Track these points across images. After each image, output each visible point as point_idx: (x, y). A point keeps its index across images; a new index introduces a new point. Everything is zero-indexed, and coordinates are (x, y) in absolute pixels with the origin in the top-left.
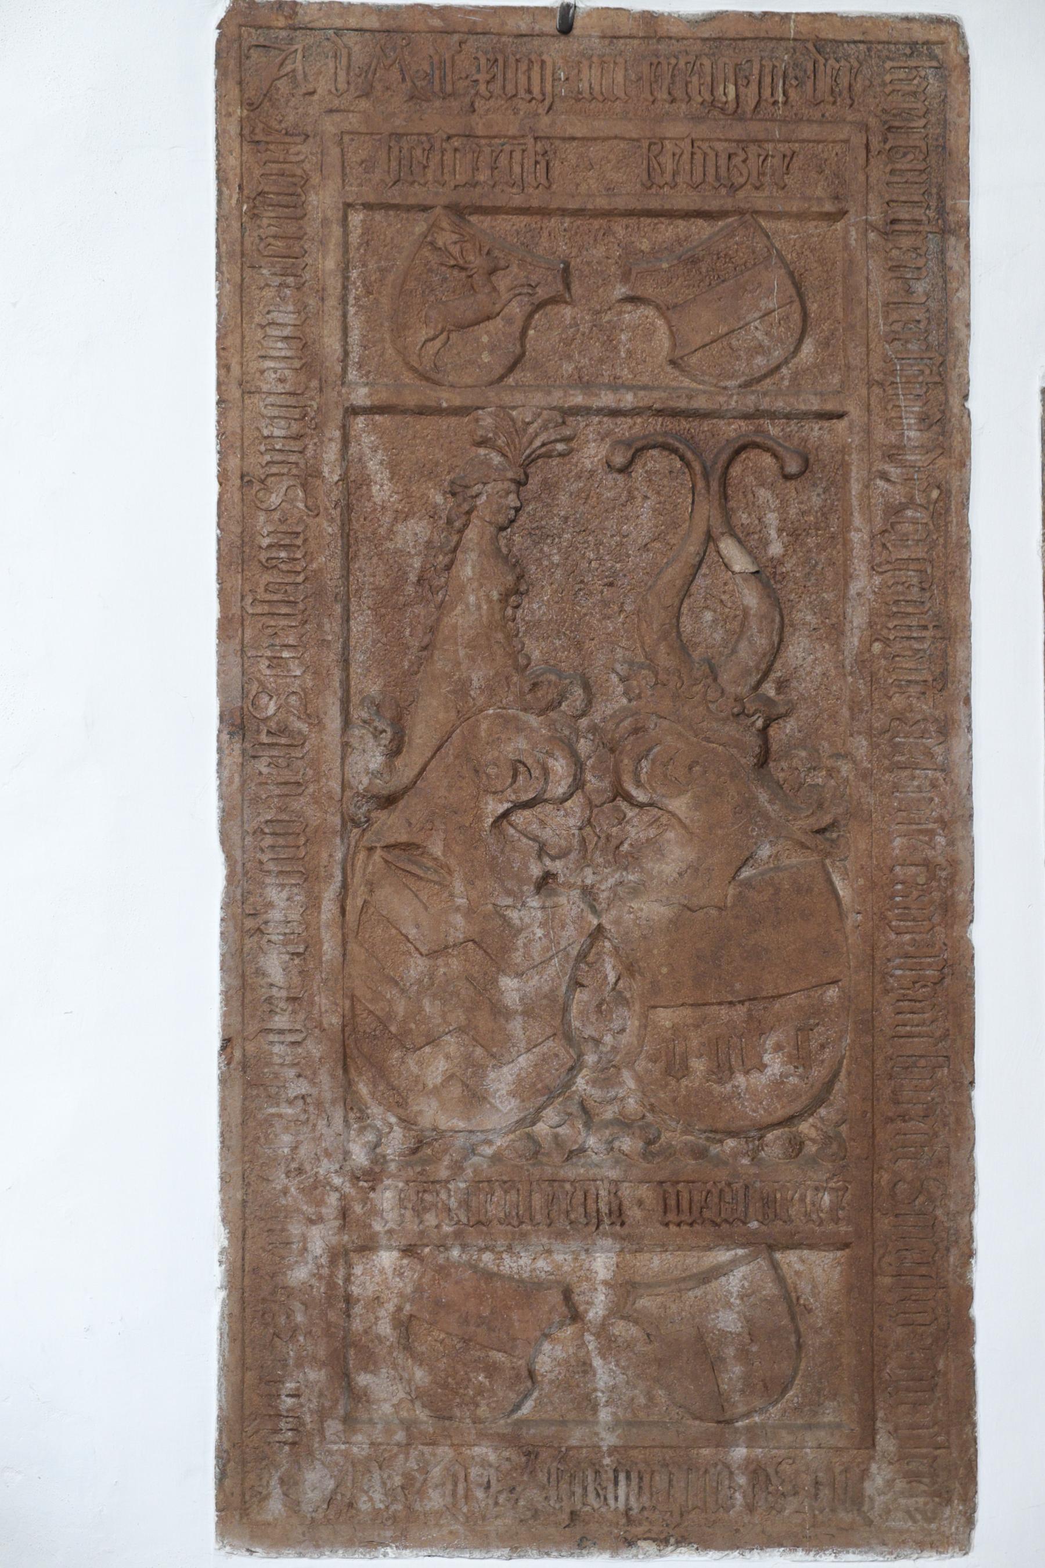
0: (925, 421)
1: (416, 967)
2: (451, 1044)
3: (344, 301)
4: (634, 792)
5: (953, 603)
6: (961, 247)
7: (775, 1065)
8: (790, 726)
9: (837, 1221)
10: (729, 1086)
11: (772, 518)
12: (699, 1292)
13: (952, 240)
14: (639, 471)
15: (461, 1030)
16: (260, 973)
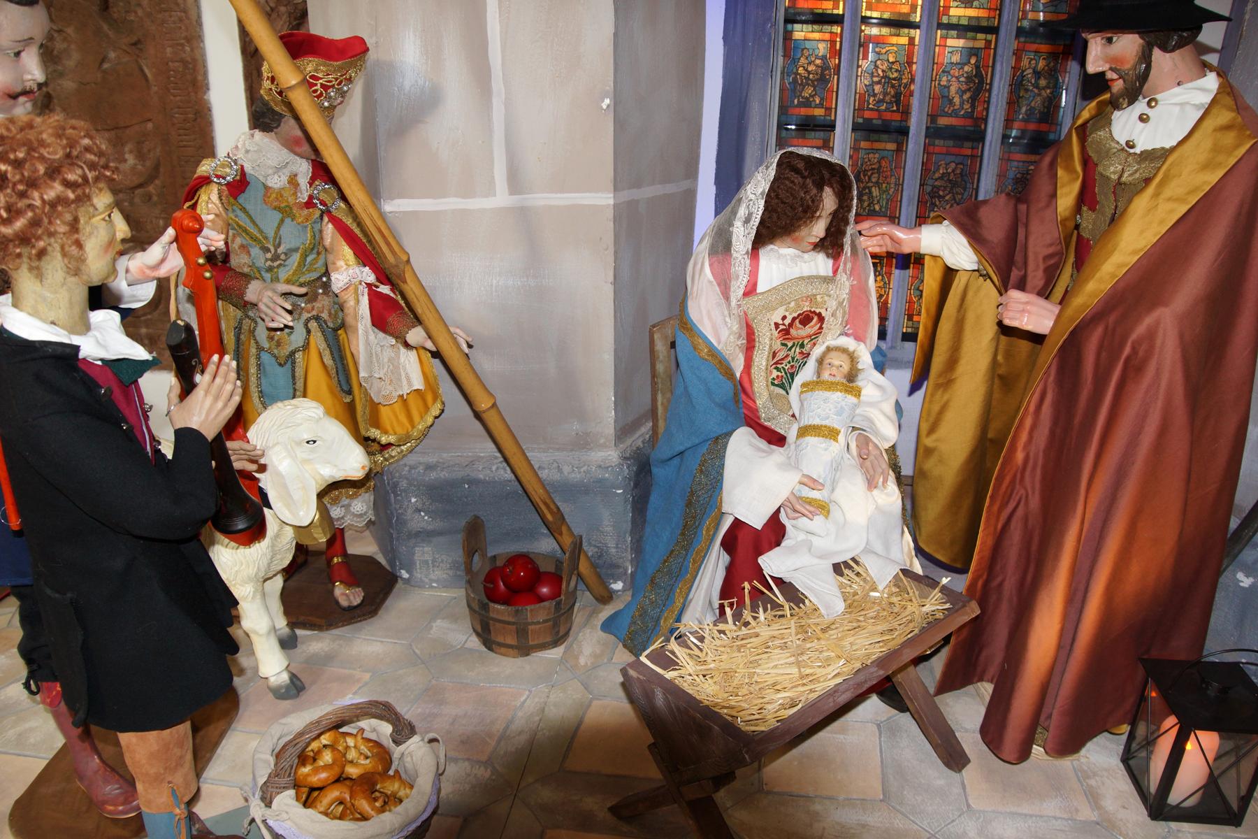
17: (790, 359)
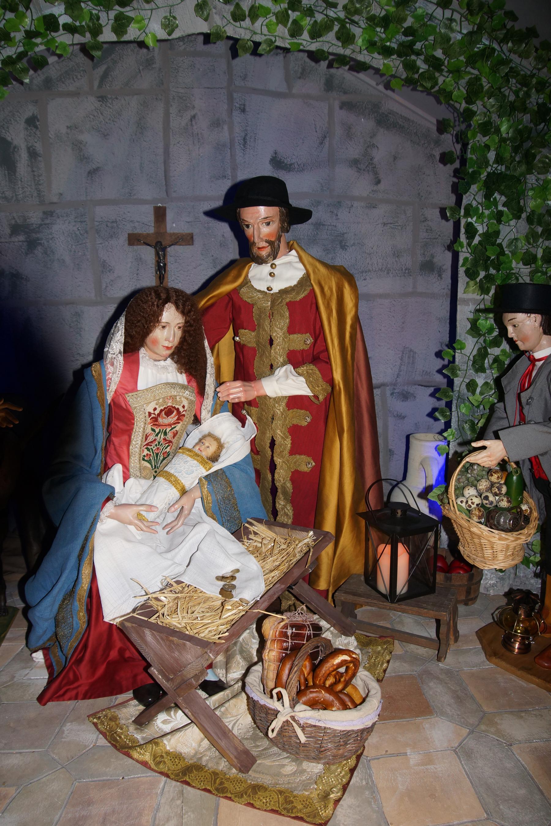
17: (157, 443)
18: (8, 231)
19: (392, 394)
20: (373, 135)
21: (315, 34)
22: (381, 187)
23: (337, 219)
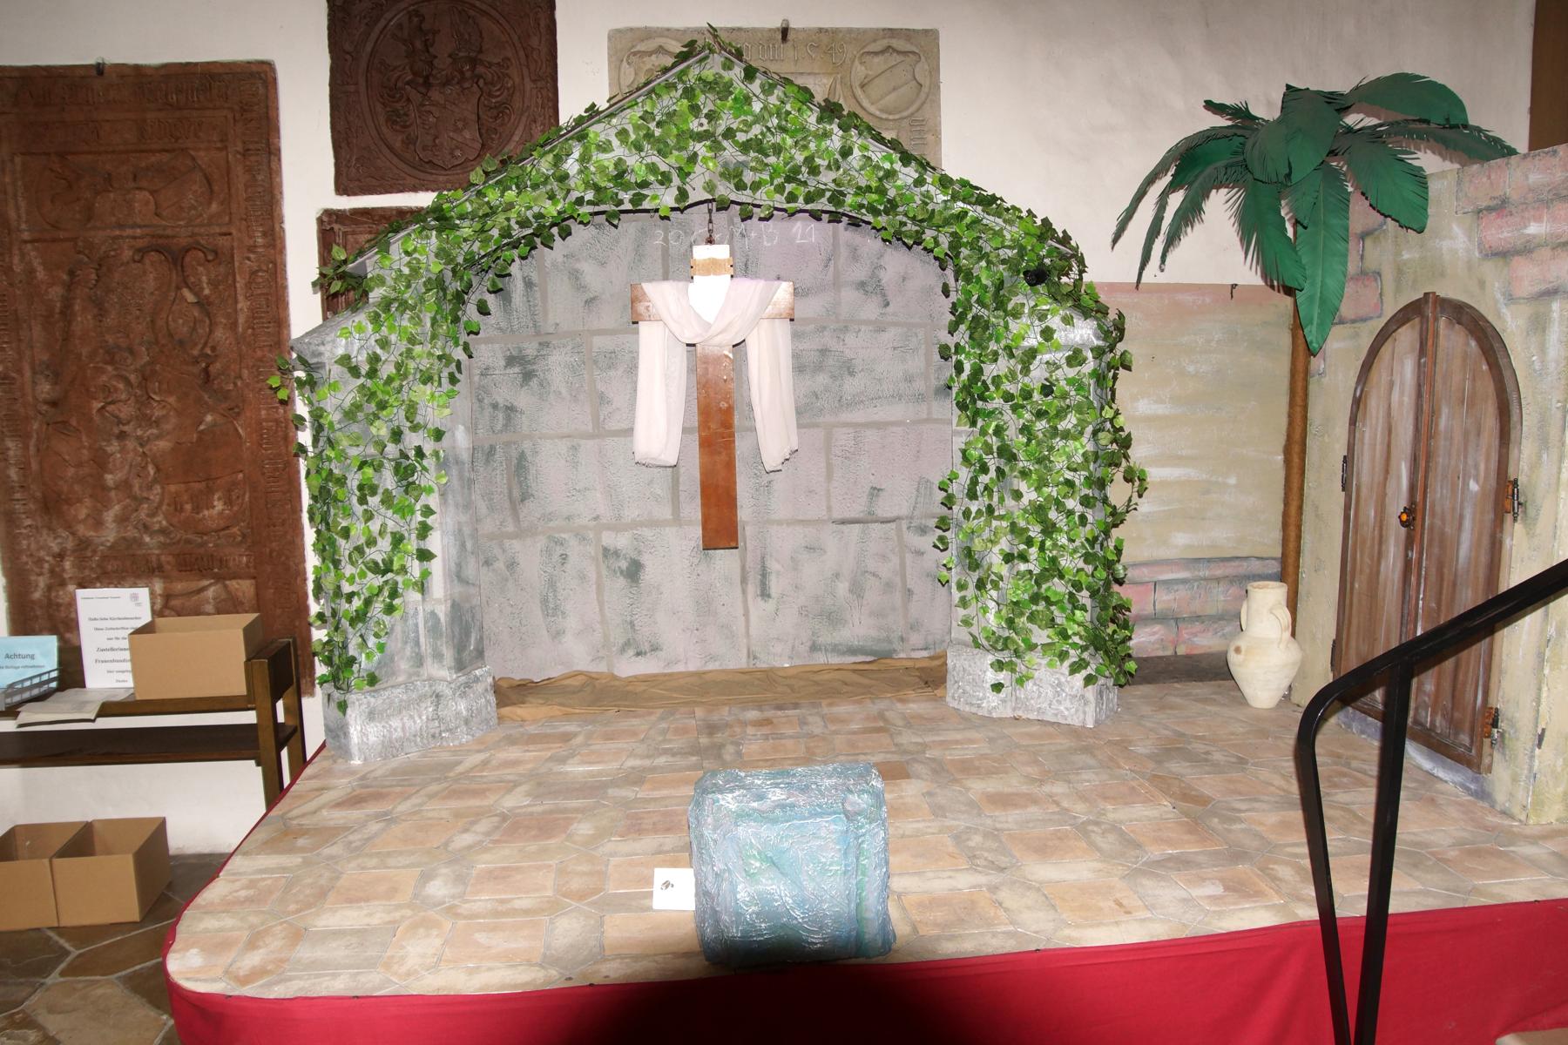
0: (265, 234)
1: (71, 471)
2: (88, 502)
3: (15, 196)
4: (154, 396)
5: (280, 311)
6: (276, 159)
7: (219, 506)
8: (218, 365)
9: (249, 567)
10: (201, 515)
11: (204, 279)
12: (196, 598)
13: (272, 157)
14: (147, 261)
15: (91, 496)
16: (9, 477)
18: (503, 363)
19: (909, 528)
20: (881, 256)
21: (809, 199)
22: (890, 309)
23: (844, 345)
